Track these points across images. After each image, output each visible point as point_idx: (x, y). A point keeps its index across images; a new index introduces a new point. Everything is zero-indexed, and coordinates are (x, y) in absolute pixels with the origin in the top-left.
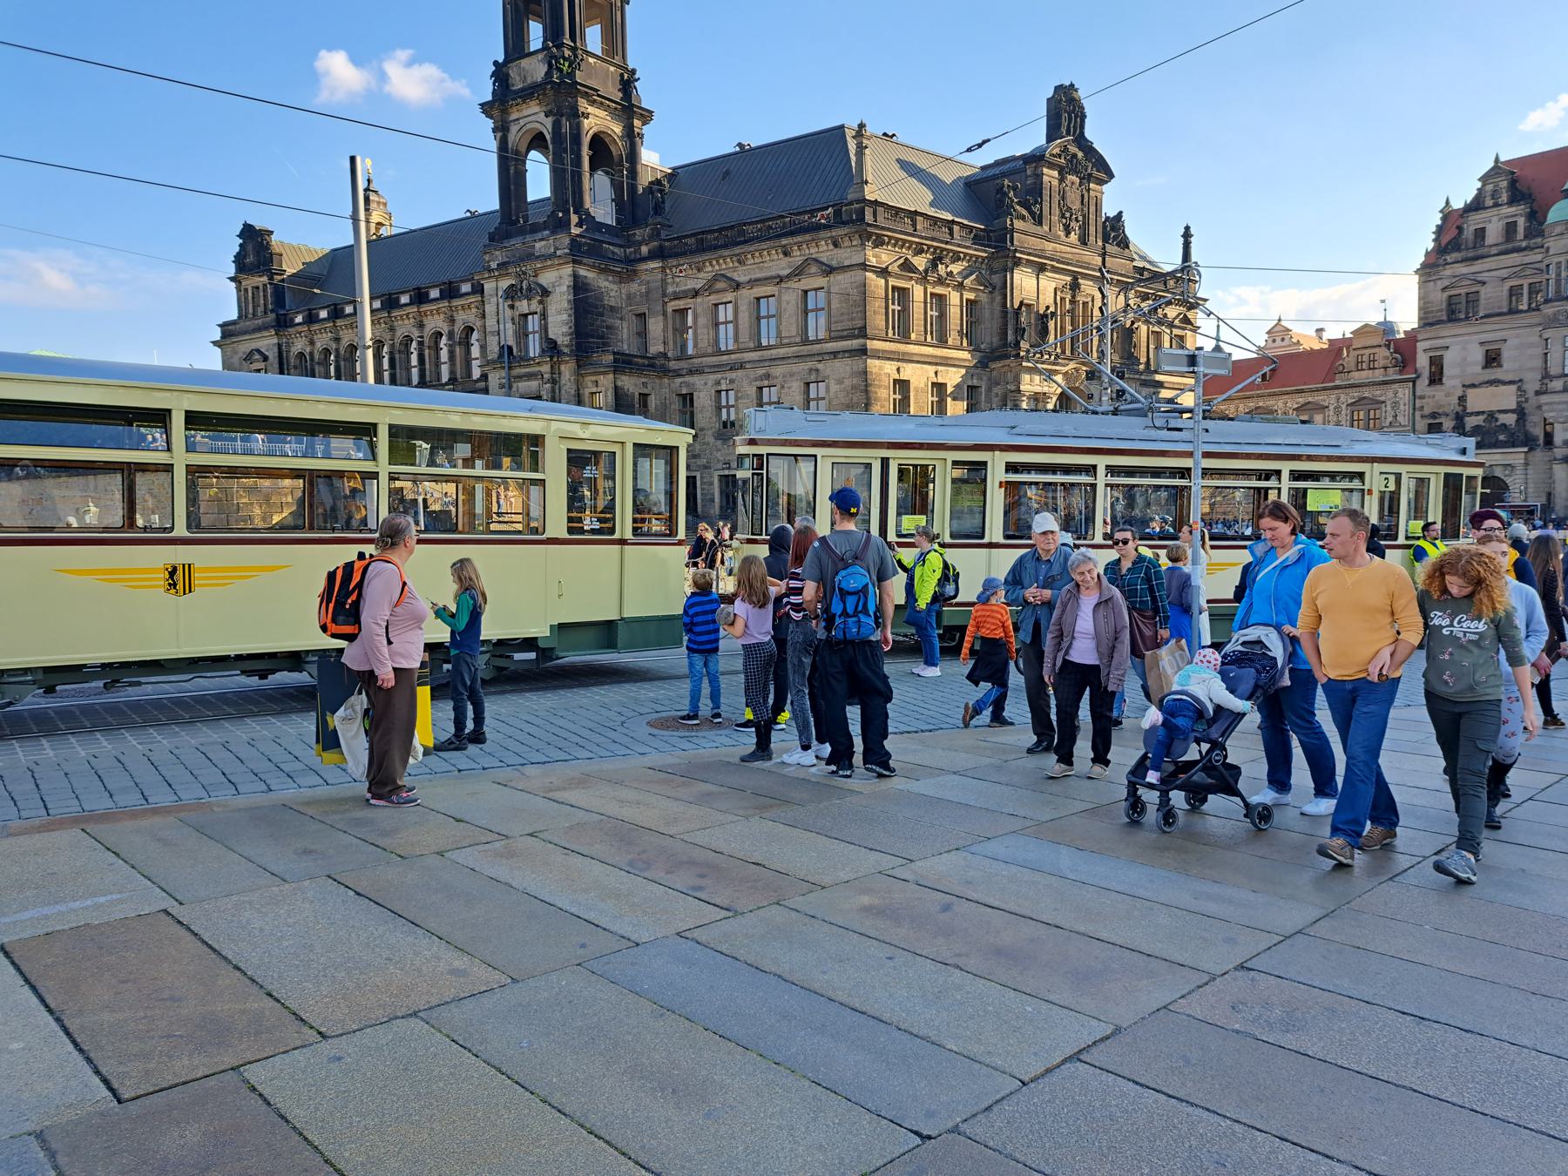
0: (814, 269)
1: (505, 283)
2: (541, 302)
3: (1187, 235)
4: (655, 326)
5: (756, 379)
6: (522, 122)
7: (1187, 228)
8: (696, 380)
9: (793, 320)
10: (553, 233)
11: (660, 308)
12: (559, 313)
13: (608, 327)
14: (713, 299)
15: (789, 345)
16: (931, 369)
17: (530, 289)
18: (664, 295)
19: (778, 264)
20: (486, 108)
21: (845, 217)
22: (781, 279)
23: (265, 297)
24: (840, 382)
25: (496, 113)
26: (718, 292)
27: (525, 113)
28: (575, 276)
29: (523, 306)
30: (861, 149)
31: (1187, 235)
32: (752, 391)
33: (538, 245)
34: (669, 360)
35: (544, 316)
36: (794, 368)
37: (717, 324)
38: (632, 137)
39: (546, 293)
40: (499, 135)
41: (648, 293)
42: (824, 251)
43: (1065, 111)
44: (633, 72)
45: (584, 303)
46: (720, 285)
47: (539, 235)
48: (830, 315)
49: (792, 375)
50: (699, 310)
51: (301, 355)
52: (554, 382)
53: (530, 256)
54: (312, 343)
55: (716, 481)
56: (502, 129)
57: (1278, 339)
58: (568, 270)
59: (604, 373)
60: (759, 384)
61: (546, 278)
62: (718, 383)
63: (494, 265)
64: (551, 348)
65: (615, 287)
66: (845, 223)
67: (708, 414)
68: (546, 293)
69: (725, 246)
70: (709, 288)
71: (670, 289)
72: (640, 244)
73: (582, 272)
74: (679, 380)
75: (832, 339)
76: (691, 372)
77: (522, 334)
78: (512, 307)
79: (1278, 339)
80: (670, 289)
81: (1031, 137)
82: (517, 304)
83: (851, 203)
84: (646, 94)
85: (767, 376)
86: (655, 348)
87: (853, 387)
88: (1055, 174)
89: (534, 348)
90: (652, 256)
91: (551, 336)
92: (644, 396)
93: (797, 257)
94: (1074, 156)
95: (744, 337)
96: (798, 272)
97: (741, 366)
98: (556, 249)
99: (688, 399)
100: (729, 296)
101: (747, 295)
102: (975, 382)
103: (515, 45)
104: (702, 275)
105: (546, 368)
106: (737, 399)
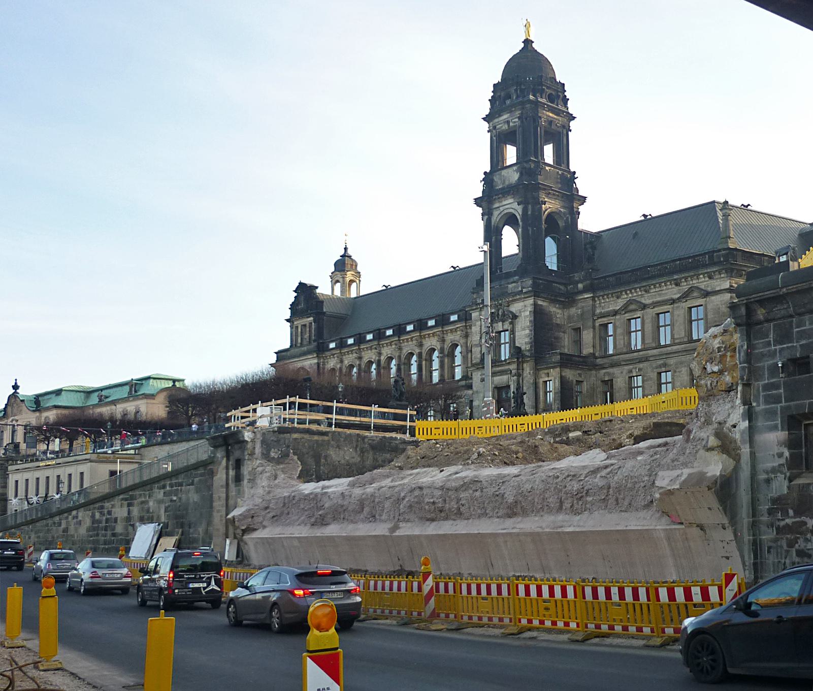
0: (695, 294)
2: (511, 323)
4: (587, 336)
5: (657, 368)
6: (501, 209)
9: (682, 327)
10: (521, 278)
11: (590, 323)
12: (524, 329)
13: (557, 338)
14: (628, 316)
17: (504, 315)
18: (594, 315)
19: (673, 292)
20: (478, 202)
21: (715, 260)
22: (673, 301)
27: (504, 203)
28: (535, 305)
29: (499, 326)
30: (726, 216)
32: (654, 376)
33: (510, 286)
34: (596, 358)
35: (513, 332)
36: (683, 358)
37: (630, 333)
39: (515, 317)
40: (486, 217)
41: (582, 314)
42: (703, 283)
44: (574, 173)
46: (632, 307)
47: (512, 280)
48: (706, 323)
49: (681, 363)
50: (618, 324)
51: (333, 369)
52: (519, 375)
54: (342, 361)
56: (487, 214)
58: (530, 301)
59: (553, 368)
60: (659, 370)
61: (515, 308)
62: (631, 371)
64: (517, 352)
65: (559, 311)
68: (515, 317)
69: (636, 281)
70: (625, 309)
71: (598, 311)
73: (540, 302)
74: (604, 371)
80: (598, 311)
83: (719, 251)
84: (582, 186)
85: (665, 365)
86: (587, 350)
91: (517, 345)
92: (579, 382)
93: (685, 287)
95: (649, 340)
96: (685, 296)
97: (646, 359)
98: (523, 288)
99: (609, 384)
100: (639, 314)
101: (651, 312)
104: (620, 300)
105: (513, 367)
106: (643, 381)
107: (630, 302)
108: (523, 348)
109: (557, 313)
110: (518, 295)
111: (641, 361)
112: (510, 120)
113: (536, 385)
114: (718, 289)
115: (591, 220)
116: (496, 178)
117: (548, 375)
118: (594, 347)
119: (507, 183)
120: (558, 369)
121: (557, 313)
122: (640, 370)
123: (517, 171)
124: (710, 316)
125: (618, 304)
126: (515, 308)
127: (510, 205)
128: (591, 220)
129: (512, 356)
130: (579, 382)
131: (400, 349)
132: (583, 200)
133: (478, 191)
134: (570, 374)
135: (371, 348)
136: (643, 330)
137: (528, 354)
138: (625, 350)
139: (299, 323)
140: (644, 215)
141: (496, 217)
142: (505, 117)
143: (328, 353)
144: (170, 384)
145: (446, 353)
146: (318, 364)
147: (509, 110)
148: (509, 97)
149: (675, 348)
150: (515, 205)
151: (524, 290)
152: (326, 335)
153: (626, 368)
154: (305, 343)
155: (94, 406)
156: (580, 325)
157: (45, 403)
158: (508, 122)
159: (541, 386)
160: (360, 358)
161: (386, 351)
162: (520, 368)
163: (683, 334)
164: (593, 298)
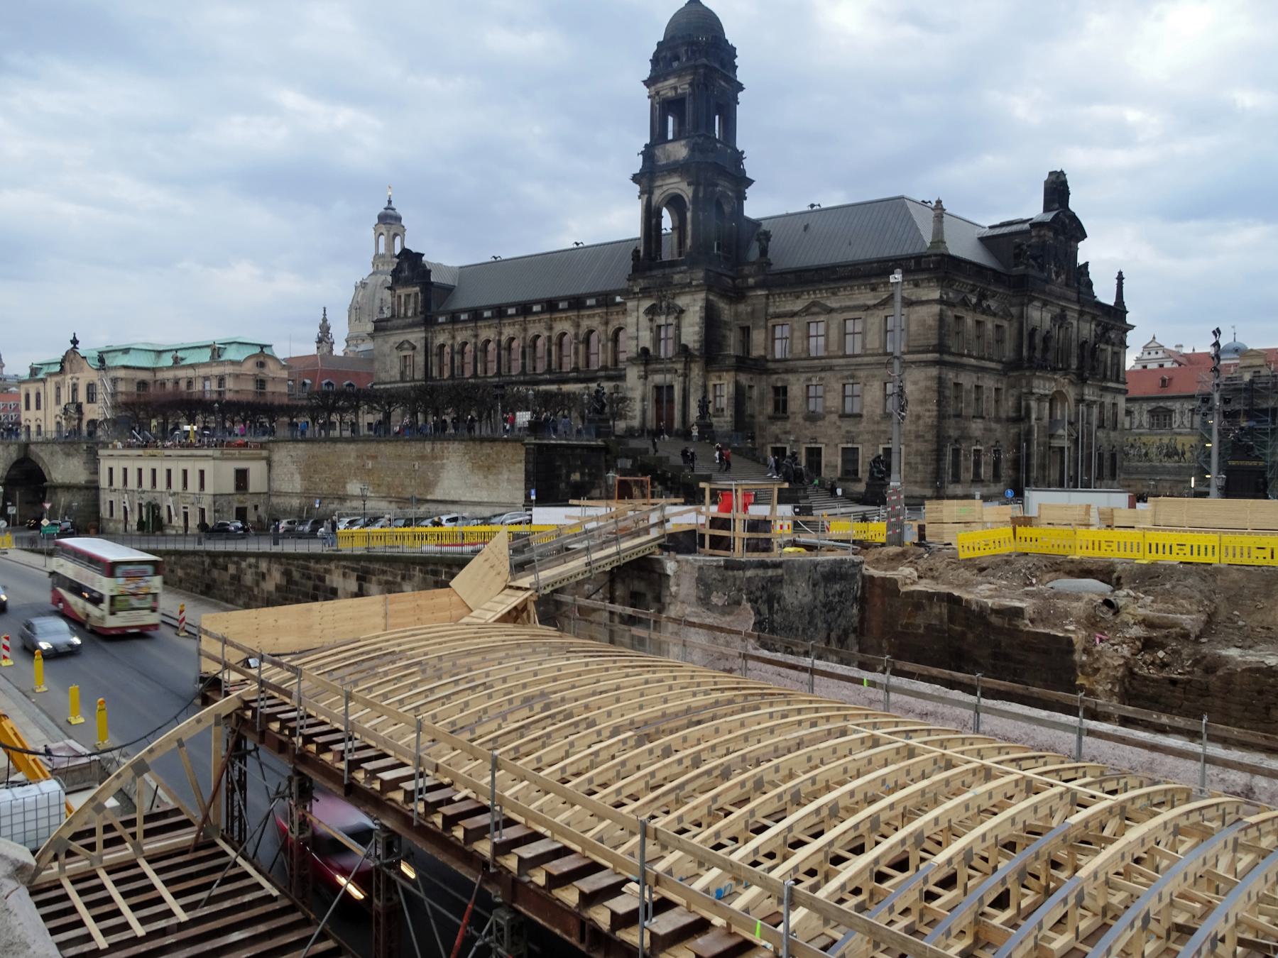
1: (647, 304)
2: (677, 318)
3: (1120, 278)
4: (758, 337)
5: (842, 378)
6: (665, 188)
7: (1120, 273)
8: (791, 378)
9: (877, 337)
11: (762, 323)
12: (692, 326)
14: (808, 319)
15: (872, 355)
16: (974, 376)
18: (766, 314)
19: (868, 298)
20: (636, 179)
21: (923, 266)
22: (867, 308)
23: (416, 303)
24: (915, 383)
25: (644, 181)
26: (813, 314)
28: (707, 300)
29: (662, 320)
31: (1120, 278)
34: (767, 361)
35: (678, 327)
36: (876, 372)
37: (809, 337)
38: (742, 197)
39: (682, 311)
40: (646, 196)
41: (753, 312)
43: (1057, 189)
45: (711, 320)
46: (815, 309)
50: (796, 326)
52: (686, 376)
53: (669, 284)
55: (803, 451)
56: (647, 192)
57: (1153, 353)
59: (727, 371)
61: (682, 301)
62: (810, 379)
63: (637, 290)
66: (923, 271)
67: (799, 402)
68: (682, 311)
69: (820, 282)
70: (806, 310)
71: (771, 310)
72: (748, 276)
73: (711, 297)
74: (775, 377)
75: (909, 353)
76: (787, 371)
77: (657, 341)
78: (651, 320)
79: (1153, 353)
80: (771, 310)
81: (1033, 208)
82: (656, 318)
86: (757, 352)
87: (927, 388)
88: (1051, 234)
89: (667, 350)
90: (757, 286)
91: (683, 342)
92: (751, 387)
94: (1063, 223)
95: (834, 348)
97: (831, 368)
101: (837, 318)
102: (999, 386)
103: (658, 135)
105: (679, 366)
106: (825, 392)
107: (814, 304)
108: (691, 346)
109: (726, 310)
110: (686, 287)
111: (823, 369)
112: (673, 86)
113: (705, 387)
114: (924, 298)
115: (756, 207)
116: (658, 152)
117: (720, 378)
118: (765, 349)
119: (672, 159)
120: (732, 374)
121: (726, 310)
122: (821, 379)
123: (685, 146)
124: (913, 328)
125: (798, 305)
126: (682, 301)
127: (677, 185)
128: (756, 207)
129: (677, 355)
130: (751, 387)
131: (525, 330)
132: (750, 182)
133: (637, 165)
134: (744, 379)
135: (490, 326)
136: (826, 336)
137: (697, 353)
138: (804, 356)
139: (402, 292)
140: (812, 206)
141: (657, 196)
142: (672, 81)
143: (438, 328)
144: (257, 350)
145: (581, 338)
146: (426, 339)
147: (679, 74)
148: (677, 58)
149: (866, 359)
150: (684, 186)
151: (694, 283)
152: (434, 308)
153: (804, 376)
154: (410, 314)
155: (169, 368)
156: (749, 323)
157: (112, 361)
158: (675, 88)
159: (711, 388)
160: (476, 336)
161: (508, 332)
162: (687, 368)
163: (877, 345)
164: (767, 297)
